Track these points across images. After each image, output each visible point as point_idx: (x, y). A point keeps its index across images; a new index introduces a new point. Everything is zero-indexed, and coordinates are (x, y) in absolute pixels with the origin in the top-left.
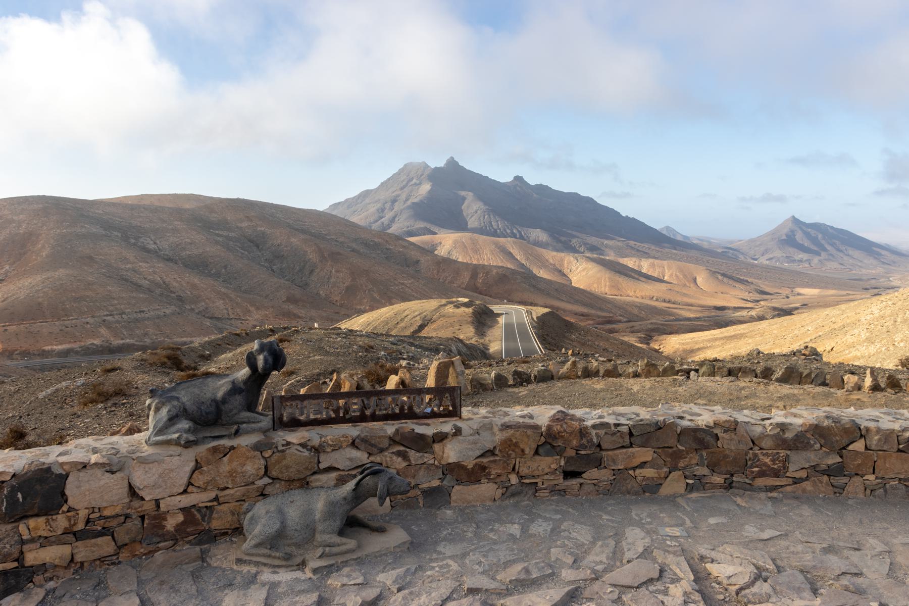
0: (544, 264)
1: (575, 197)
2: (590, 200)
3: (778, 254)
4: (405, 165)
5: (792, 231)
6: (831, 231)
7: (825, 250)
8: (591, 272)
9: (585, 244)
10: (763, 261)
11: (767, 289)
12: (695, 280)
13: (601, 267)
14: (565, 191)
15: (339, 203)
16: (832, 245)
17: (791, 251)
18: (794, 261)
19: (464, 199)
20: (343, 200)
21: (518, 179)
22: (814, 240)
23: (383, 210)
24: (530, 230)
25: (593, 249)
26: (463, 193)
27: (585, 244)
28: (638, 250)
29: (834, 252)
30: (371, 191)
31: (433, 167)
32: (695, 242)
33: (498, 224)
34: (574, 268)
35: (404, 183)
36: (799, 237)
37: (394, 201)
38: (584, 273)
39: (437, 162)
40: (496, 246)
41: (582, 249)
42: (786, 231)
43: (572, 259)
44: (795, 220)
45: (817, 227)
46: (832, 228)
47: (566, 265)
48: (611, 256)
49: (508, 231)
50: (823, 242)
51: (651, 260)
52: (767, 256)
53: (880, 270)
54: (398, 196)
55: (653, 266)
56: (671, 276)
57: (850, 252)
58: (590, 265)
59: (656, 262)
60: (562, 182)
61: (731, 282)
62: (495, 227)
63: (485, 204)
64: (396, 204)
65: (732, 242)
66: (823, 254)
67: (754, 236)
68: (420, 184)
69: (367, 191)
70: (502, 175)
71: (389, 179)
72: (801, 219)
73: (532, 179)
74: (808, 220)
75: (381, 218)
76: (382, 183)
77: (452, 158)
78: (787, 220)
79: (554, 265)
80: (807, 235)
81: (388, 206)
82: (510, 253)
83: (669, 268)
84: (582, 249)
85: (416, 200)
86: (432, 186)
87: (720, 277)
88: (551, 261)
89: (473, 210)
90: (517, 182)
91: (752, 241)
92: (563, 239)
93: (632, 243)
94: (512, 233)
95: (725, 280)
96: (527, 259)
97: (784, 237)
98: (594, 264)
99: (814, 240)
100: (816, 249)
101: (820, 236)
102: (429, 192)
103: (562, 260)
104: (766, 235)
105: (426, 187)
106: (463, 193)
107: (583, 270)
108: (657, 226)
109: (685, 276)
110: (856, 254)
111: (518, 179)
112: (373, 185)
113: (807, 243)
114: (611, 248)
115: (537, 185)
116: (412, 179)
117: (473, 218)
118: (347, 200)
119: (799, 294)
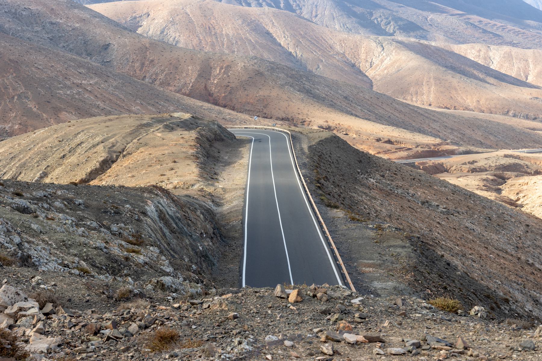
9: (397, 19)
25: (409, 27)
28: (485, 31)
34: (376, 61)
40: (244, 21)
41: (390, 29)
43: (374, 44)
47: (363, 56)
48: (438, 42)
51: (506, 49)
55: (509, 57)
59: (515, 51)
79: (344, 54)
82: (268, 33)
84: (390, 29)
88: (338, 48)
92: (359, 10)
93: (475, 18)
96: (297, 44)
98: (412, 55)
103: (357, 47)
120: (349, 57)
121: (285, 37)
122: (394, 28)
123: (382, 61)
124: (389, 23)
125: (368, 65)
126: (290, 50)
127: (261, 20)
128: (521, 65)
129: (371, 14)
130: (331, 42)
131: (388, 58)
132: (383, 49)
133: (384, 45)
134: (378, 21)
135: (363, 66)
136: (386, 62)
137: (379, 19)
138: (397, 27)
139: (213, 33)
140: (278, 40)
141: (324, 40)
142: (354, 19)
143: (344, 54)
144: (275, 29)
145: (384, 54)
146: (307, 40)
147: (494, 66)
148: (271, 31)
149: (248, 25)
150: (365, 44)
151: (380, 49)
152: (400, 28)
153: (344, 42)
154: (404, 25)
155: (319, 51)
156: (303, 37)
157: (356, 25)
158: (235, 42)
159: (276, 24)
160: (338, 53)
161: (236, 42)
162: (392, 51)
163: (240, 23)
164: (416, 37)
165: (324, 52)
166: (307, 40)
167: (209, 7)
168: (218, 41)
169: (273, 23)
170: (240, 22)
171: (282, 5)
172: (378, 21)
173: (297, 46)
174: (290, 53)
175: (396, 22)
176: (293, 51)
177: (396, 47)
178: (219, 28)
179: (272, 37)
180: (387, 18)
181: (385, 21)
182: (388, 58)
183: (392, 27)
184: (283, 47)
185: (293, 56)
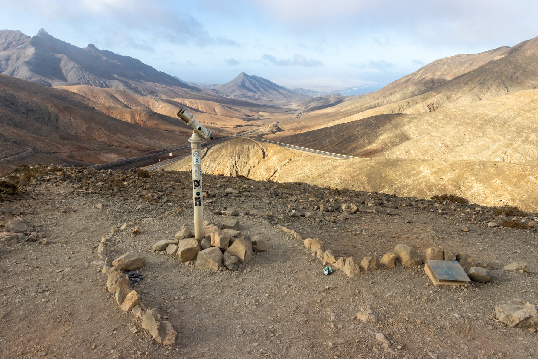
0: (138, 104)
1: (128, 58)
3: (238, 93)
5: (244, 80)
6: (261, 80)
7: (259, 90)
8: (167, 109)
9: (147, 90)
10: (232, 97)
11: (248, 114)
12: (215, 110)
13: (172, 106)
14: (123, 55)
16: (263, 87)
17: (245, 91)
18: (247, 97)
19: (61, 60)
21: (91, 46)
22: (254, 85)
24: (111, 81)
25: (152, 93)
26: (59, 55)
27: (147, 90)
28: (176, 93)
29: (264, 92)
31: (32, 36)
32: (192, 85)
33: (89, 77)
34: (156, 107)
35: (5, 45)
36: (247, 84)
38: (163, 109)
39: (31, 32)
40: (106, 93)
42: (240, 80)
44: (244, 74)
45: (254, 77)
46: (261, 78)
47: (151, 105)
49: (98, 82)
50: (258, 86)
51: (190, 100)
52: (233, 94)
53: (285, 101)
54: (10, 56)
55: (191, 103)
56: (202, 108)
57: (271, 92)
58: (166, 104)
59: (193, 100)
60: (122, 50)
61: (232, 111)
62: (88, 79)
63: (78, 63)
64: (10, 61)
65: (210, 86)
66: (258, 92)
67: (225, 82)
68: (25, 48)
70: (82, 43)
72: (248, 74)
74: (250, 74)
77: (42, 29)
78: (240, 74)
80: (250, 82)
83: (201, 104)
84: (145, 93)
85: (26, 60)
86: (36, 49)
87: (227, 108)
89: (68, 67)
90: (91, 48)
91: (224, 85)
94: (100, 83)
95: (229, 110)
96: (128, 101)
97: (240, 84)
98: (168, 104)
99: (254, 85)
100: (254, 89)
101: (257, 83)
102: (35, 54)
103: (148, 102)
104: (231, 82)
105: (31, 51)
106: (59, 55)
107: (163, 107)
108: (172, 76)
109: (209, 108)
110: (274, 92)
111: (91, 46)
113: (251, 87)
114: (161, 92)
115: (104, 50)
116: (12, 42)
117: (71, 73)
119: (262, 116)
123: (158, 106)
128: (196, 105)
135: (152, 109)
147: (187, 105)
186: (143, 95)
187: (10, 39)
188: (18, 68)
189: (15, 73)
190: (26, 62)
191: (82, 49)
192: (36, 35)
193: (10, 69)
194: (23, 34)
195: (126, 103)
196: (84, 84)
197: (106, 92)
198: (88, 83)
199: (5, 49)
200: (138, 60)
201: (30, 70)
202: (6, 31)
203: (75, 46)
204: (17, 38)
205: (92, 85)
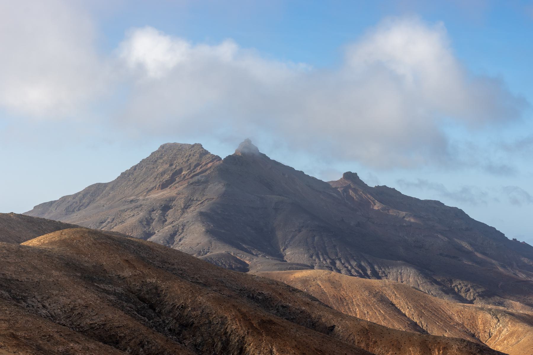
0: (447, 321)
1: (435, 206)
2: (459, 214)
4: (162, 147)
8: (524, 340)
15: (51, 203)
20: (57, 198)
21: (351, 177)
23: (148, 221)
30: (106, 185)
34: (494, 332)
35: (167, 177)
37: (166, 207)
40: (370, 292)
41: (470, 296)
43: (489, 316)
47: (481, 327)
49: (354, 263)
54: (172, 199)
58: (520, 327)
64: (170, 212)
68: (206, 182)
69: (99, 184)
71: (135, 168)
73: (372, 178)
75: (150, 235)
76: (122, 174)
79: (463, 324)
81: (156, 215)
82: (393, 305)
84: (470, 296)
88: (456, 318)
90: (348, 182)
94: (360, 266)
98: (528, 327)
103: (473, 319)
107: (511, 335)
112: (109, 175)
115: (378, 187)
116: (181, 170)
118: (64, 199)
120: (468, 327)
121: (408, 308)
122: (474, 294)
123: (500, 332)
124: (469, 290)
125: (486, 335)
126: (415, 320)
127: (385, 292)
129: (451, 283)
130: (449, 313)
131: (505, 330)
132: (499, 321)
133: (498, 317)
134: (458, 288)
135: (483, 337)
136: (503, 332)
137: (459, 287)
138: (477, 294)
139: (345, 304)
140: (402, 310)
141: (443, 311)
142: (437, 286)
143: (463, 324)
144: (398, 301)
145: (501, 325)
146: (429, 311)
148: (395, 302)
149: (374, 297)
150: (481, 316)
151: (496, 321)
152: (479, 296)
153: (461, 314)
154: (482, 292)
155: (441, 321)
156: (424, 308)
157: (440, 292)
158: (366, 312)
159: (398, 296)
160: (458, 324)
161: (368, 312)
162: (508, 323)
163: (367, 294)
164: (494, 304)
165: (446, 322)
166: (429, 311)
167: (337, 279)
168: (351, 311)
169: (395, 295)
170: (367, 293)
171: (369, 272)
172: (458, 288)
173: (421, 317)
174: (416, 323)
175: (475, 290)
176: (418, 322)
177: (510, 319)
178: (349, 299)
179: (396, 308)
180: (466, 286)
181: (464, 288)
182: (505, 330)
183: (472, 294)
184: (409, 318)
185: (418, 326)
186: (463, 300)
187: (180, 162)
188: (184, 226)
189: (177, 238)
190: (201, 214)
191: (327, 185)
192: (232, 153)
193: (167, 229)
194: (207, 152)
195: (415, 320)
196: (321, 267)
197: (370, 289)
198: (332, 266)
199: (164, 186)
200: (461, 212)
201: (209, 232)
202: (175, 145)
203: (314, 179)
204: (193, 160)
205: (339, 271)
